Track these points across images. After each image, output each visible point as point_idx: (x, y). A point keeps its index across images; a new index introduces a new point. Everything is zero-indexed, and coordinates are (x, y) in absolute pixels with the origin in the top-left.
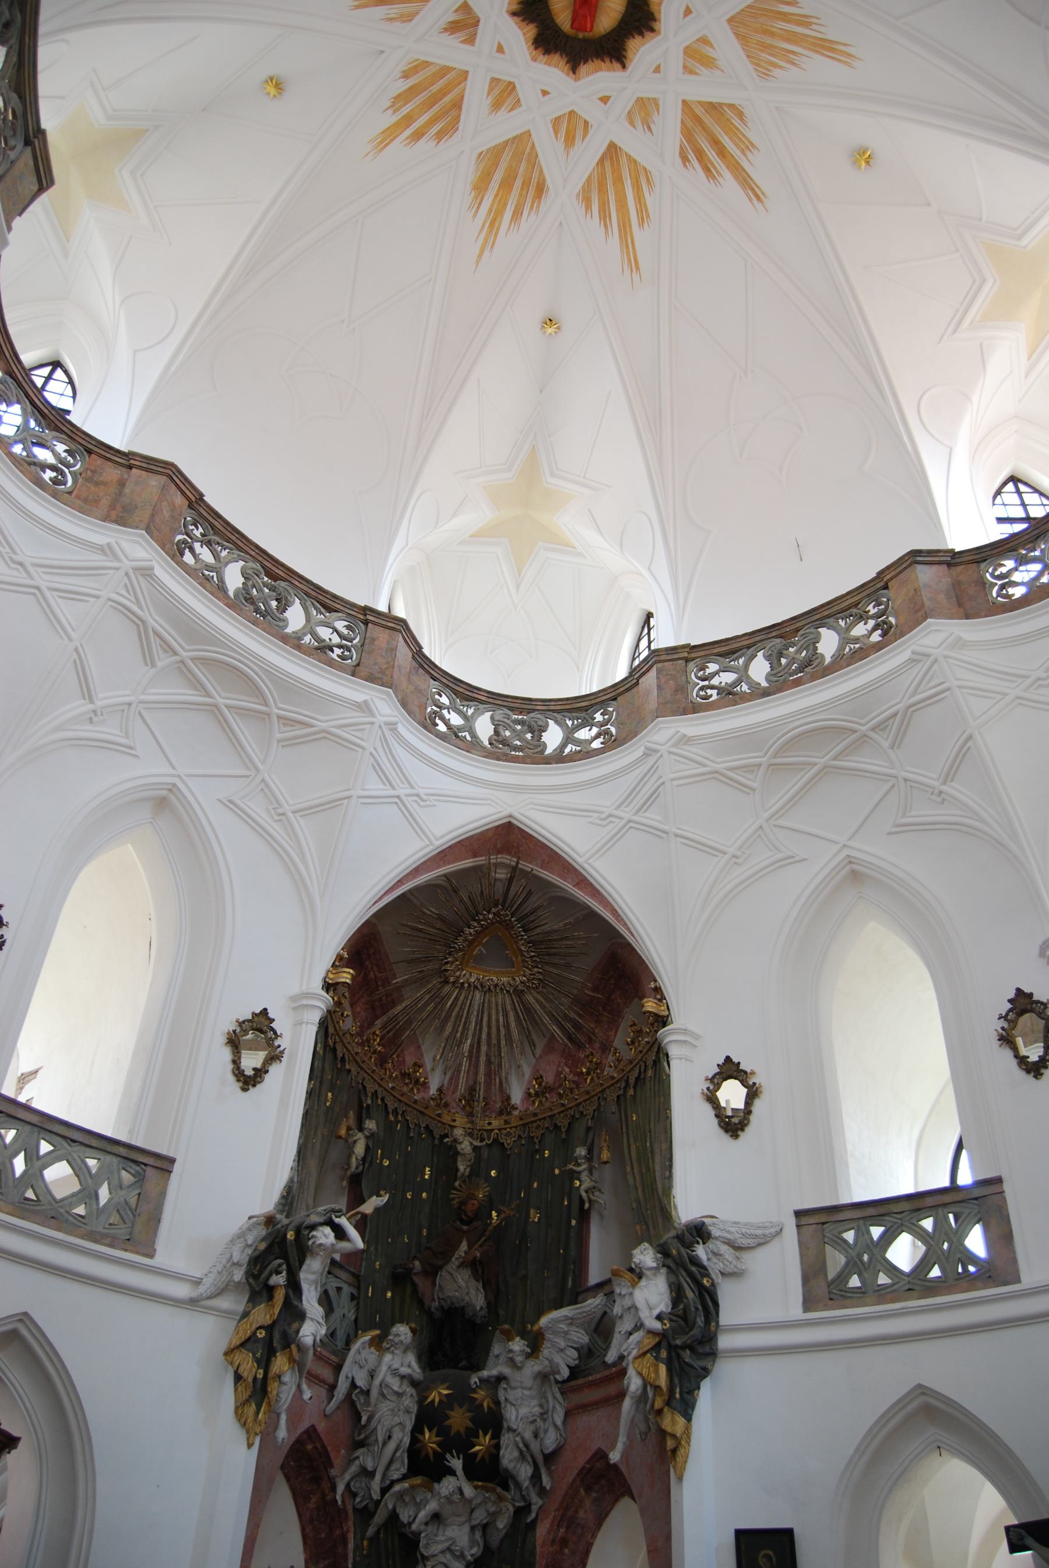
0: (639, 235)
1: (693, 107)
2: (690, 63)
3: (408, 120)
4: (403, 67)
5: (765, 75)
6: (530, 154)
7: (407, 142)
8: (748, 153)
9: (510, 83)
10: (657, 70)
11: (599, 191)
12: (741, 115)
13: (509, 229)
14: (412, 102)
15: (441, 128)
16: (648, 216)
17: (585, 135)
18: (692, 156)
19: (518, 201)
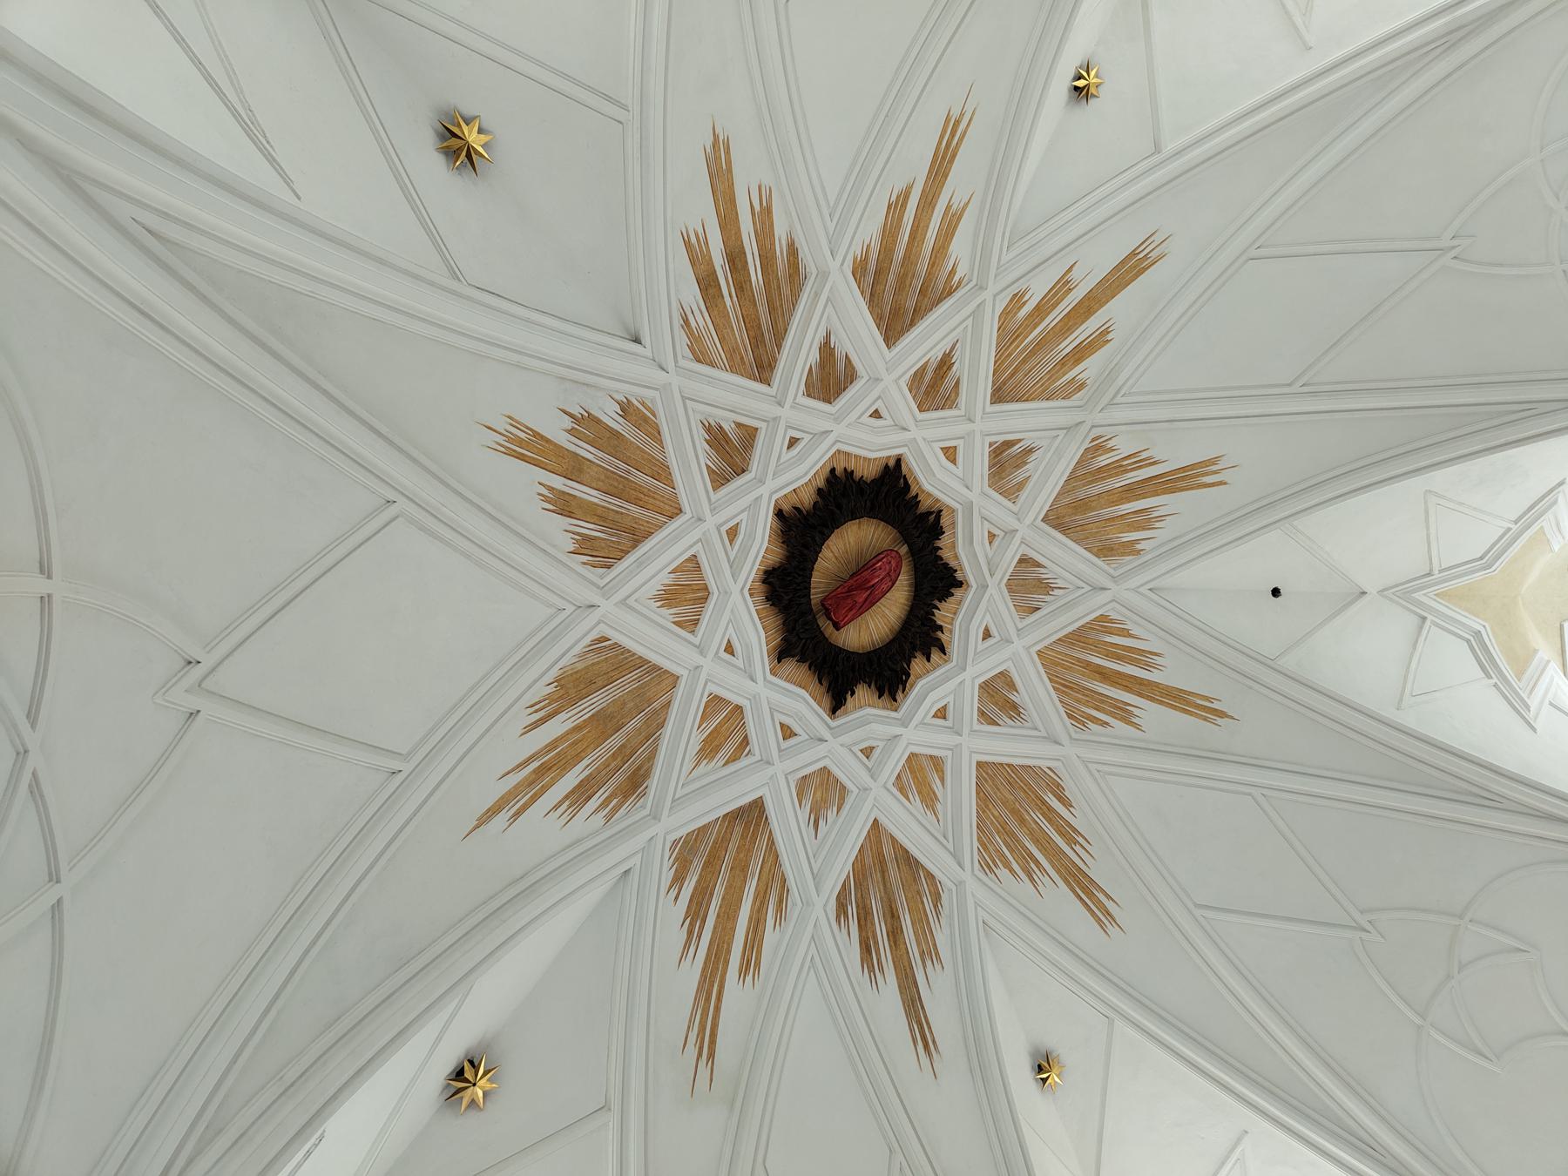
0: (736, 994)
1: (884, 840)
2: (908, 778)
3: (574, 468)
4: (634, 393)
5: (987, 867)
6: (655, 712)
7: (546, 492)
8: (929, 963)
9: (706, 588)
10: (867, 752)
11: (708, 864)
12: (937, 899)
13: (556, 807)
14: (600, 454)
15: (596, 538)
16: (758, 964)
17: (733, 759)
18: (852, 910)
19: (598, 771)
